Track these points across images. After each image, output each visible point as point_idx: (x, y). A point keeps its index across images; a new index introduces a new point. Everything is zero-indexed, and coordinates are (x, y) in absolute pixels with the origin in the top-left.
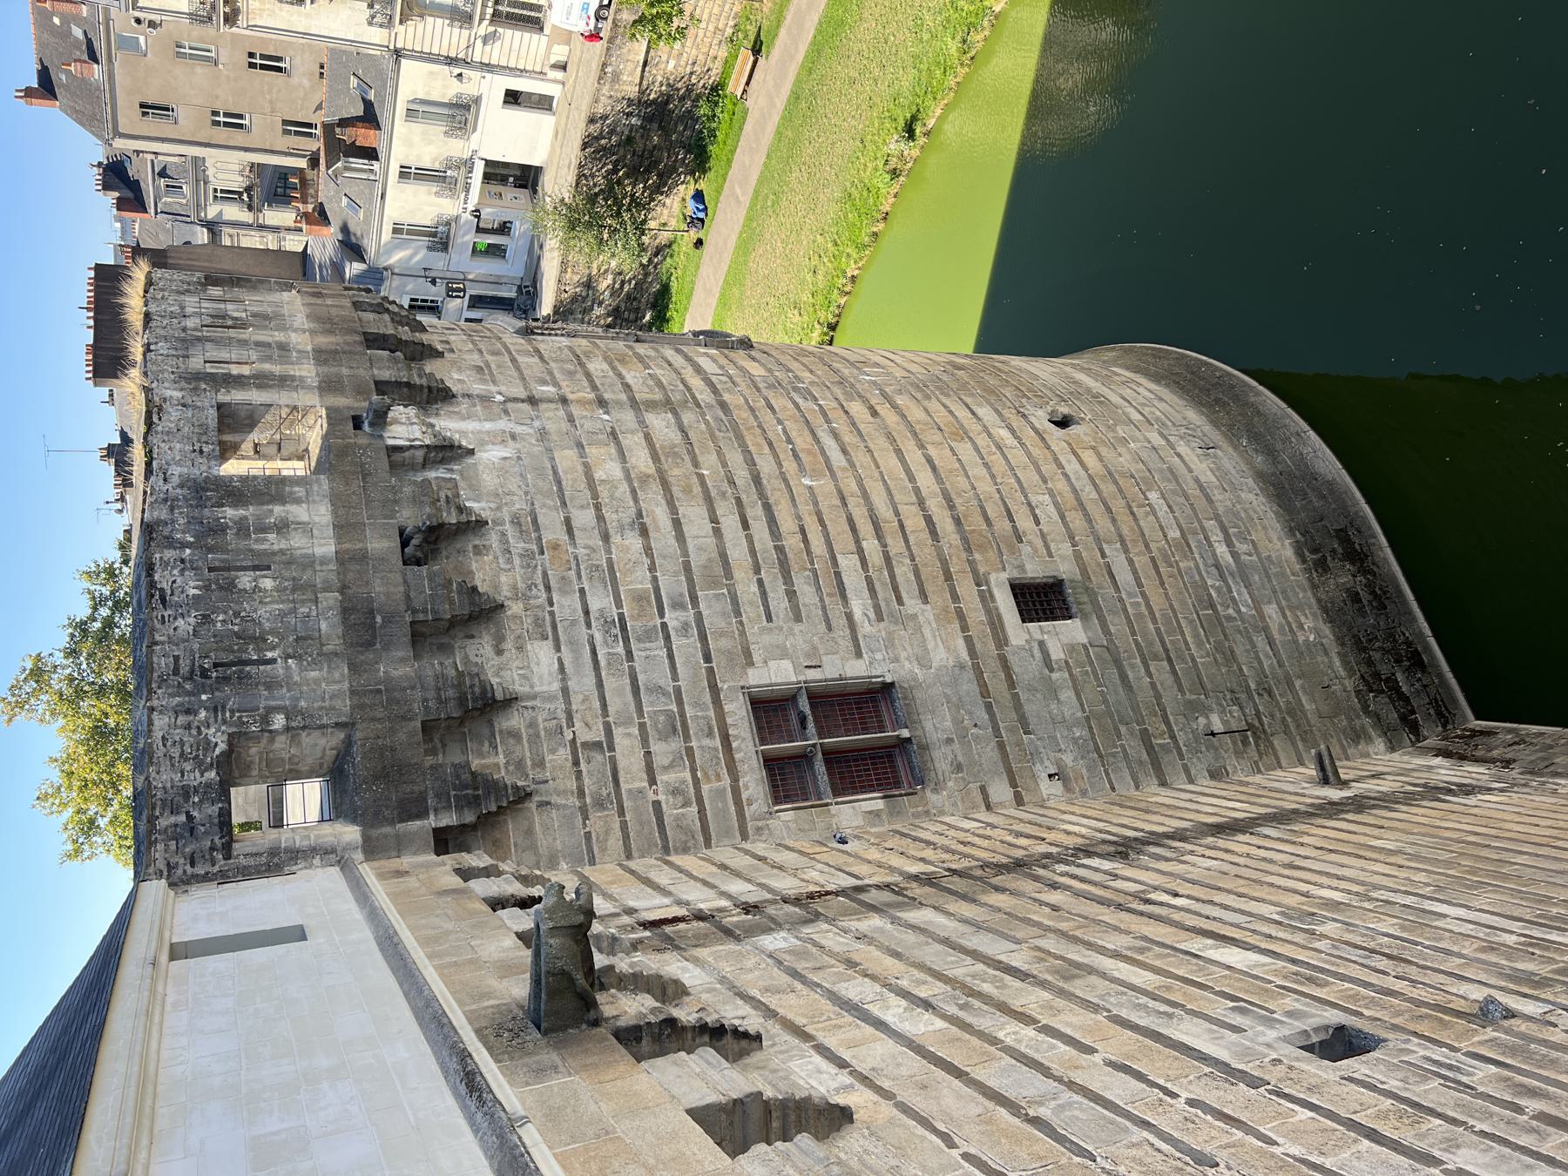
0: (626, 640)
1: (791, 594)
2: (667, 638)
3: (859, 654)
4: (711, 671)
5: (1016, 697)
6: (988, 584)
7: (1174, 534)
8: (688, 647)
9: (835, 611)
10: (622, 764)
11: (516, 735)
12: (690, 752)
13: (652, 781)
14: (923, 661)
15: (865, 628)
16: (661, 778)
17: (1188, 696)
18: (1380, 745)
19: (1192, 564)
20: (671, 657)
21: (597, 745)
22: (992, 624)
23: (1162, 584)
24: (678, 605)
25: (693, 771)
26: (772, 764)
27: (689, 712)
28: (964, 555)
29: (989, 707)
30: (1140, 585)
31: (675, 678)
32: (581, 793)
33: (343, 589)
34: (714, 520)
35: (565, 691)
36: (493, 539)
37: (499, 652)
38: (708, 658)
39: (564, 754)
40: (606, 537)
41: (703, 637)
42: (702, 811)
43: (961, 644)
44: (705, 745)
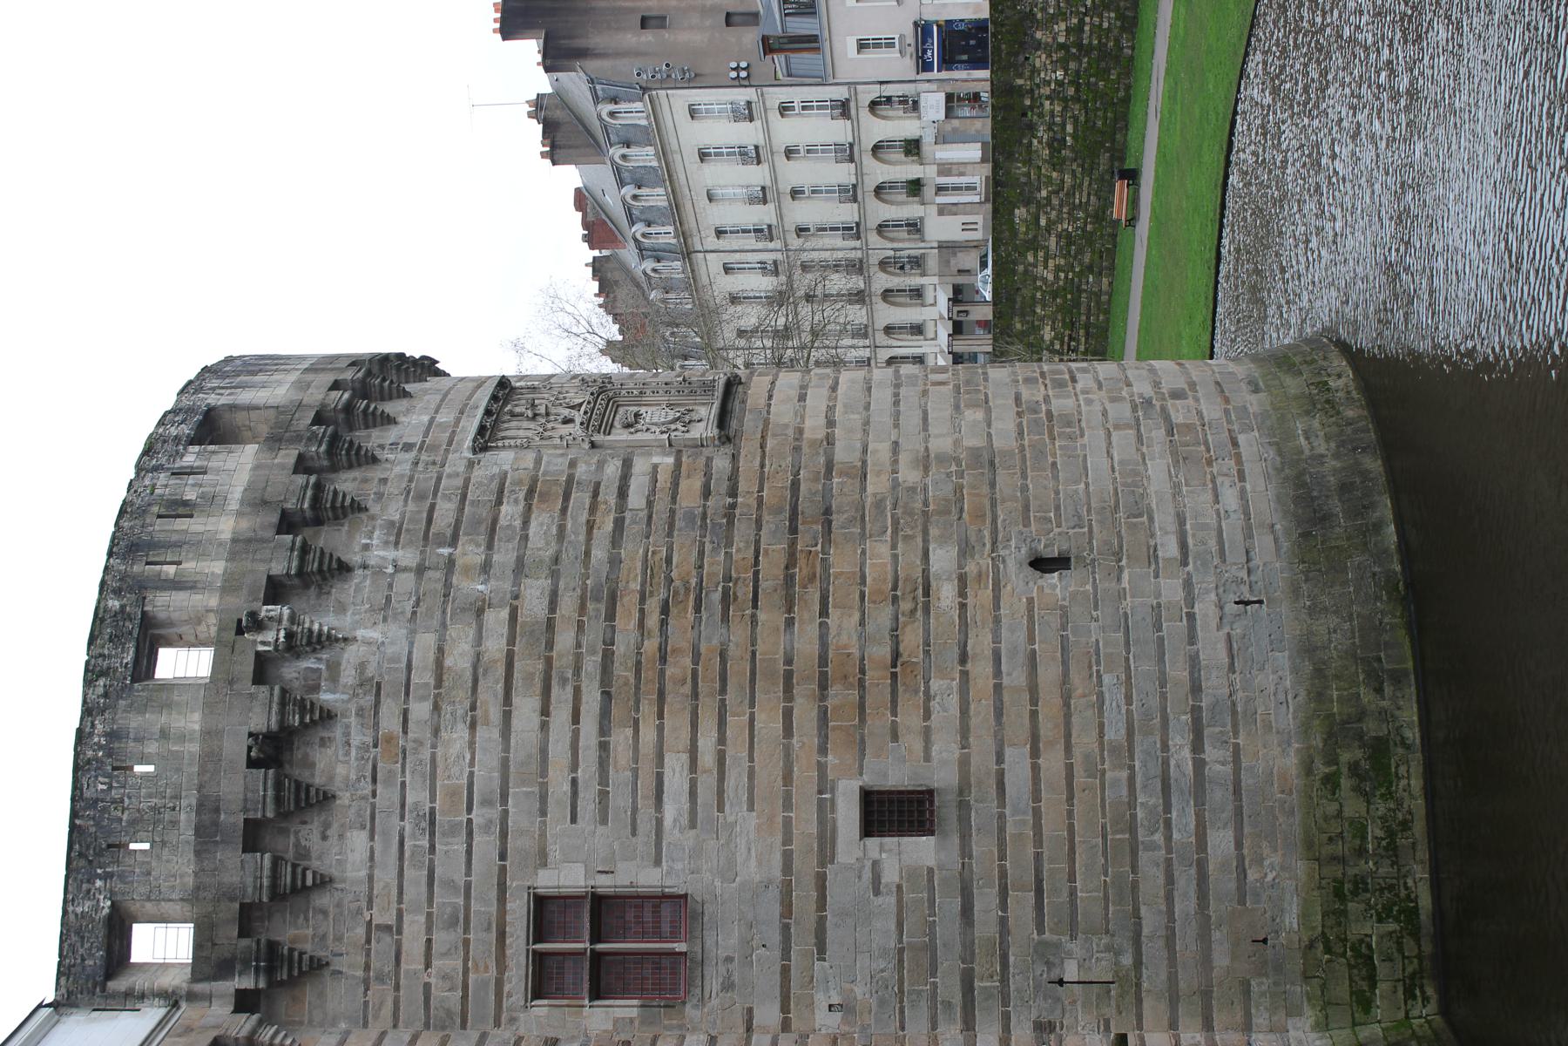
0: (432, 834)
1: (603, 795)
2: (470, 834)
3: (658, 862)
4: (503, 870)
5: (821, 924)
6: (833, 791)
7: (1115, 732)
8: (485, 845)
9: (646, 812)
10: (405, 948)
11: (325, 913)
12: (466, 943)
13: (428, 965)
14: (728, 871)
15: (671, 833)
16: (435, 963)
17: (1047, 936)
18: (1310, 1016)
19: (1125, 774)
20: (469, 852)
21: (388, 928)
22: (821, 837)
23: (1070, 798)
24: (487, 802)
25: (466, 960)
26: (539, 959)
27: (474, 906)
28: (815, 757)
29: (786, 929)
30: (1037, 798)
31: (468, 873)
32: (367, 967)
33: (200, 788)
34: (545, 711)
35: (371, 878)
36: (338, 732)
37: (324, 838)
38: (503, 856)
39: (361, 931)
40: (436, 732)
41: (504, 835)
42: (465, 997)
43: (777, 859)
44: (483, 940)
